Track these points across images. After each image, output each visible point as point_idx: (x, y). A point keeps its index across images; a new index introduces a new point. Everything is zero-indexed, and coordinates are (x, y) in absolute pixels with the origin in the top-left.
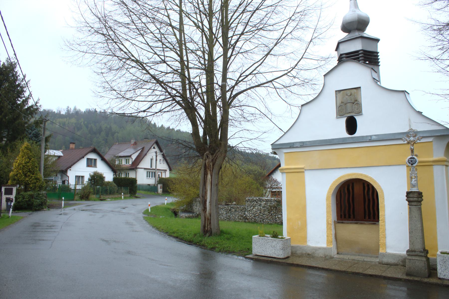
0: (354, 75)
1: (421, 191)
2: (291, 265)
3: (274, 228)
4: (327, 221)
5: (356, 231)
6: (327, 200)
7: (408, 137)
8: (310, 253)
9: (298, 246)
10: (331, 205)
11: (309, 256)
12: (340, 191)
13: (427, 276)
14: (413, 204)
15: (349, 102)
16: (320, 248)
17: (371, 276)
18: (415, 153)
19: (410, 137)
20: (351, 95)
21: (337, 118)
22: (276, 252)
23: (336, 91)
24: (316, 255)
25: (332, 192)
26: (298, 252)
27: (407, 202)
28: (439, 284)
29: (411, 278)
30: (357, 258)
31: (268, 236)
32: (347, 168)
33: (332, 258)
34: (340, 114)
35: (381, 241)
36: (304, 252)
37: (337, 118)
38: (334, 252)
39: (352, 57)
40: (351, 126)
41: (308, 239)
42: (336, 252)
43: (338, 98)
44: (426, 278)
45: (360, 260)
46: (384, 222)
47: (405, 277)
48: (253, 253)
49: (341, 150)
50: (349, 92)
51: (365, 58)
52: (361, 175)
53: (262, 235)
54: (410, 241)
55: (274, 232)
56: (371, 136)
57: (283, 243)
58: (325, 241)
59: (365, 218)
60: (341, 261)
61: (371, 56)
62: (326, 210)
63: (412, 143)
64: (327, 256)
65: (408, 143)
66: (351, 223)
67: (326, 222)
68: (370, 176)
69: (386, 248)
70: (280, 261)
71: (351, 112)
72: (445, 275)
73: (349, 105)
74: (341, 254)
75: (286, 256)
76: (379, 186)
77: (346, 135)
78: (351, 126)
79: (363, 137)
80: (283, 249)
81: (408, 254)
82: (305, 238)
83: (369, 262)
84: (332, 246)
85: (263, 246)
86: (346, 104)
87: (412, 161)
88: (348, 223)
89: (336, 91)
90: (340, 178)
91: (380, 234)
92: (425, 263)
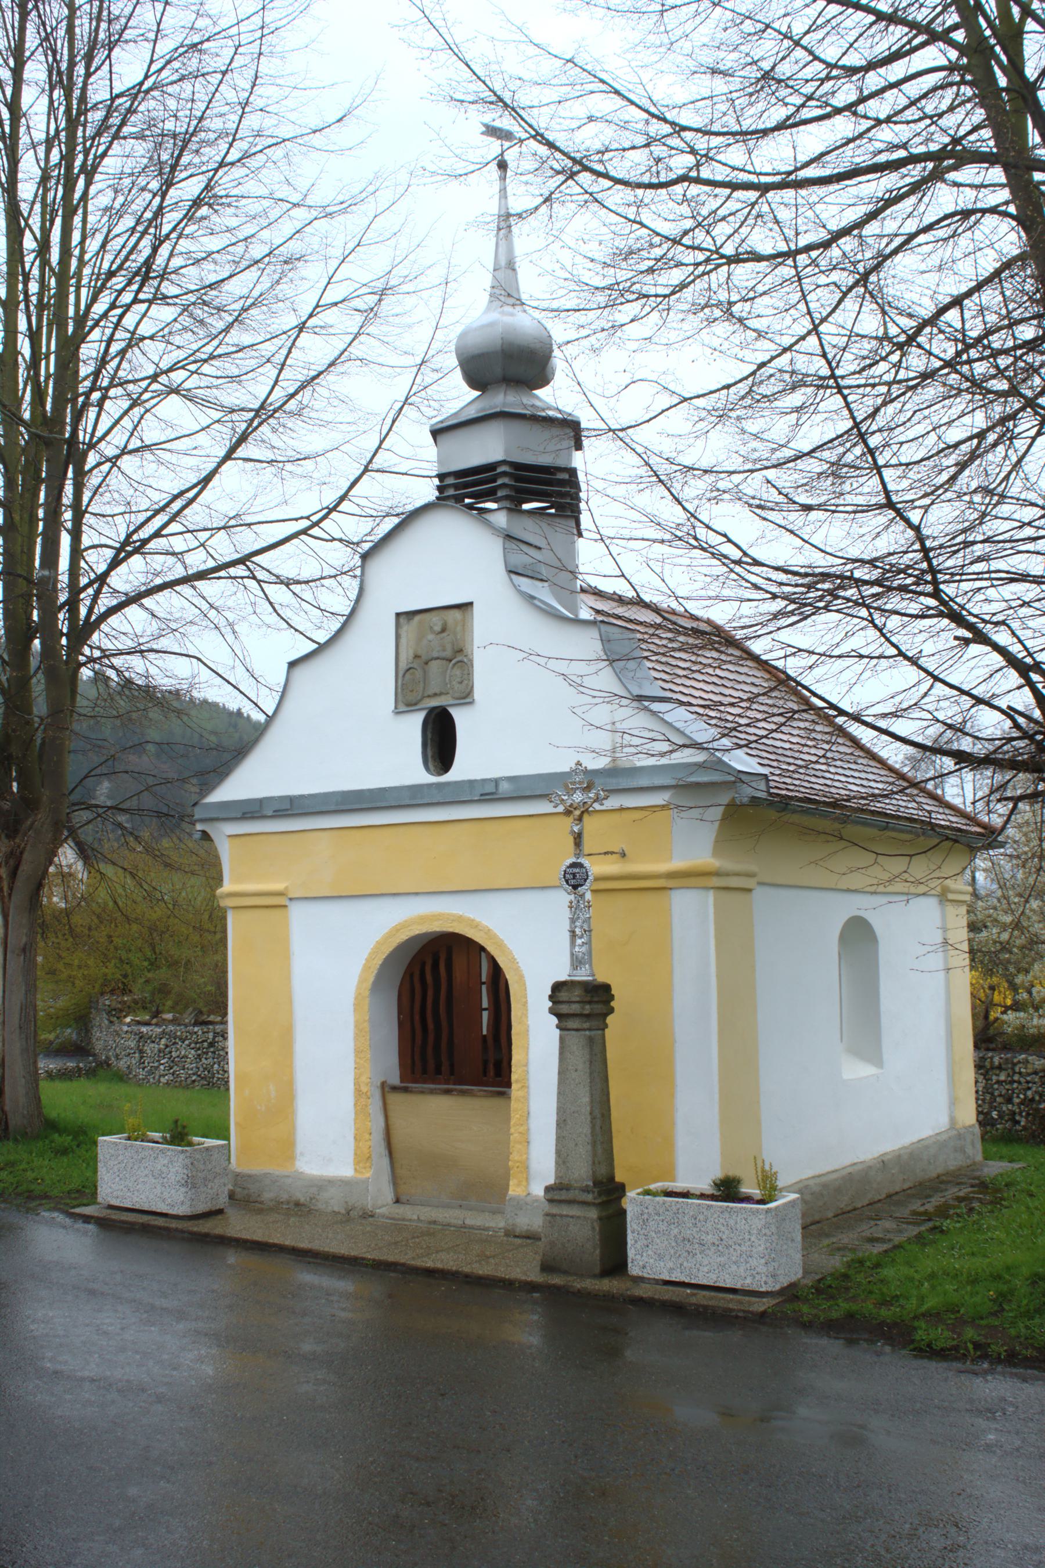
0: (461, 560)
1: (601, 978)
2: (222, 1237)
3: (182, 1105)
4: (357, 1083)
5: (443, 1117)
6: (357, 1006)
7: (570, 792)
8: (302, 1200)
9: (265, 1174)
10: (366, 1025)
11: (299, 1209)
12: (412, 976)
13: (597, 1270)
14: (572, 1024)
15: (435, 654)
16: (331, 1182)
17: (430, 1272)
18: (588, 846)
19: (575, 790)
20: (443, 630)
21: (397, 712)
22: (166, 1195)
23: (398, 615)
24: (321, 1206)
25: (372, 979)
26: (267, 1196)
27: (554, 1020)
28: (589, 1293)
29: (557, 1280)
30: (453, 1216)
31: (157, 1135)
32: (417, 894)
33: (367, 1215)
34: (405, 702)
35: (515, 1156)
36: (285, 1197)
37: (397, 712)
38: (380, 1195)
39: (465, 488)
40: (440, 741)
41: (299, 1148)
42: (389, 1196)
43: (403, 641)
44: (595, 1276)
45: (453, 1221)
46: (525, 1087)
47: (535, 1276)
48: (100, 1199)
49: (402, 829)
50: (436, 620)
51: (518, 490)
52: (460, 919)
53: (137, 1135)
54: (558, 1153)
55: (176, 1122)
56: (496, 781)
57: (188, 1161)
58: (351, 1158)
59: (485, 1074)
60: (397, 1226)
61: (549, 483)
62: (352, 1044)
63: (577, 813)
64: (353, 1208)
65: (568, 813)
66: (432, 1092)
67: (351, 1087)
68: (485, 923)
69: (527, 1179)
70: (174, 1224)
71: (441, 694)
72: (644, 1267)
73: (434, 665)
74: (408, 1202)
75: (202, 1208)
76: (513, 960)
77: (424, 777)
78: (440, 741)
79: (471, 783)
80: (191, 1183)
81: (549, 1196)
82: (288, 1147)
83: (479, 1228)
84: (368, 1174)
85: (136, 1173)
86: (426, 663)
87: (574, 875)
88: (422, 1092)
89: (398, 615)
90: (396, 930)
91: (512, 1130)
92: (593, 1228)
